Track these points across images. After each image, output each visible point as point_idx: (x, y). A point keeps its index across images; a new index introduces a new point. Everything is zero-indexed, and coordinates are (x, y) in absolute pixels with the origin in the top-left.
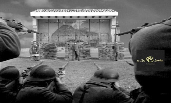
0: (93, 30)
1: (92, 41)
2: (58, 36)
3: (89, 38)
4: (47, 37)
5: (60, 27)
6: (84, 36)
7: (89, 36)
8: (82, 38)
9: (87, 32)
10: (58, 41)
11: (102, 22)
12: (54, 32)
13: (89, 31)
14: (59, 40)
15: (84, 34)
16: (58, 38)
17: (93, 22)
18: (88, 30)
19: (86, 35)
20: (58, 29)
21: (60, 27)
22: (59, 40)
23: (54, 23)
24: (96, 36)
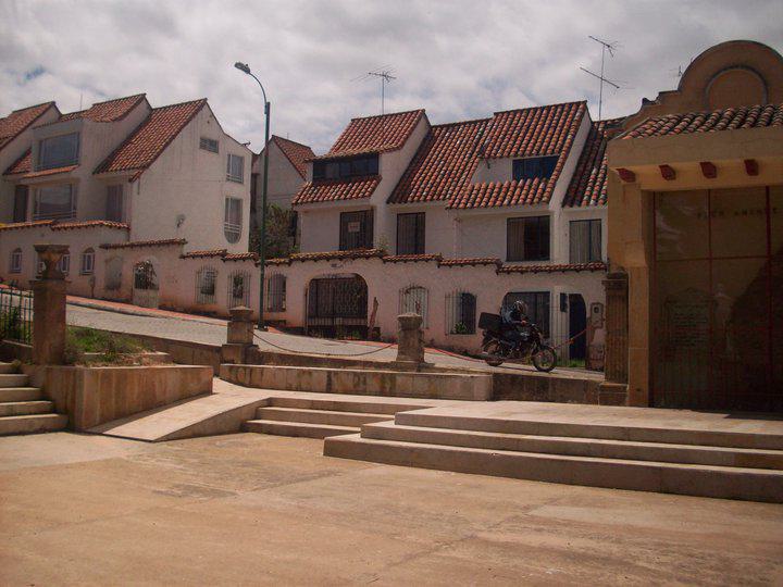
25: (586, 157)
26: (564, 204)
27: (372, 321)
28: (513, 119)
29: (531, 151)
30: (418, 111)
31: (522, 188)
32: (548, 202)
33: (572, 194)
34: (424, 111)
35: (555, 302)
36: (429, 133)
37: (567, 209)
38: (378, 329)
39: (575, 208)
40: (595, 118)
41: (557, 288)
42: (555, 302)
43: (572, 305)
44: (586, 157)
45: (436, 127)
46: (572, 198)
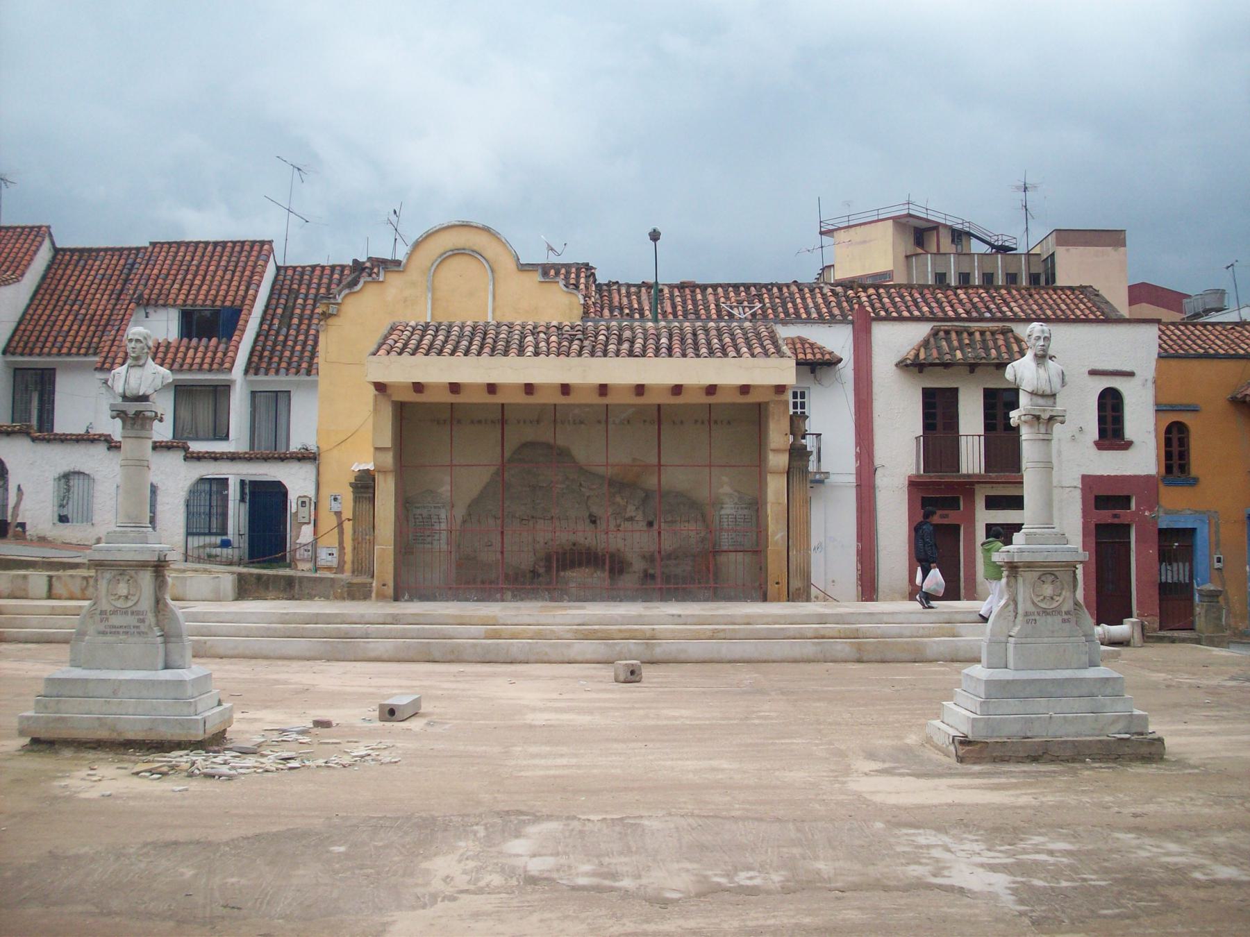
0: (677, 478)
1: (669, 557)
2: (499, 522)
3: (656, 534)
4: (443, 526)
5: (507, 454)
6: (628, 524)
7: (656, 526)
8: (620, 535)
9: (647, 496)
10: (499, 556)
11: (729, 423)
12: (475, 492)
13: (656, 488)
14: (502, 553)
15: (631, 510)
16: (499, 538)
17: (682, 422)
18: (651, 482)
19: (639, 517)
20: (492, 470)
21: (507, 454)
22: (502, 553)
23: (480, 422)
24: (692, 526)
25: (271, 312)
26: (246, 372)
27: (15, 514)
28: (177, 253)
29: (202, 299)
30: (40, 227)
31: (196, 349)
32: (230, 370)
33: (255, 359)
34: (48, 227)
35: (233, 491)
36: (54, 258)
37: (252, 377)
38: (23, 525)
39: (261, 377)
40: (280, 264)
41: (234, 474)
42: (233, 491)
43: (252, 494)
44: (271, 312)
45: (64, 250)
46: (252, 367)
